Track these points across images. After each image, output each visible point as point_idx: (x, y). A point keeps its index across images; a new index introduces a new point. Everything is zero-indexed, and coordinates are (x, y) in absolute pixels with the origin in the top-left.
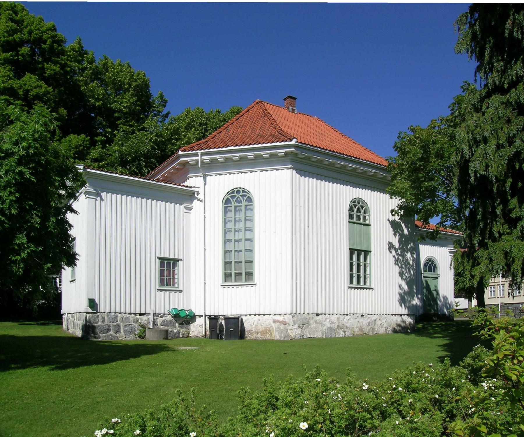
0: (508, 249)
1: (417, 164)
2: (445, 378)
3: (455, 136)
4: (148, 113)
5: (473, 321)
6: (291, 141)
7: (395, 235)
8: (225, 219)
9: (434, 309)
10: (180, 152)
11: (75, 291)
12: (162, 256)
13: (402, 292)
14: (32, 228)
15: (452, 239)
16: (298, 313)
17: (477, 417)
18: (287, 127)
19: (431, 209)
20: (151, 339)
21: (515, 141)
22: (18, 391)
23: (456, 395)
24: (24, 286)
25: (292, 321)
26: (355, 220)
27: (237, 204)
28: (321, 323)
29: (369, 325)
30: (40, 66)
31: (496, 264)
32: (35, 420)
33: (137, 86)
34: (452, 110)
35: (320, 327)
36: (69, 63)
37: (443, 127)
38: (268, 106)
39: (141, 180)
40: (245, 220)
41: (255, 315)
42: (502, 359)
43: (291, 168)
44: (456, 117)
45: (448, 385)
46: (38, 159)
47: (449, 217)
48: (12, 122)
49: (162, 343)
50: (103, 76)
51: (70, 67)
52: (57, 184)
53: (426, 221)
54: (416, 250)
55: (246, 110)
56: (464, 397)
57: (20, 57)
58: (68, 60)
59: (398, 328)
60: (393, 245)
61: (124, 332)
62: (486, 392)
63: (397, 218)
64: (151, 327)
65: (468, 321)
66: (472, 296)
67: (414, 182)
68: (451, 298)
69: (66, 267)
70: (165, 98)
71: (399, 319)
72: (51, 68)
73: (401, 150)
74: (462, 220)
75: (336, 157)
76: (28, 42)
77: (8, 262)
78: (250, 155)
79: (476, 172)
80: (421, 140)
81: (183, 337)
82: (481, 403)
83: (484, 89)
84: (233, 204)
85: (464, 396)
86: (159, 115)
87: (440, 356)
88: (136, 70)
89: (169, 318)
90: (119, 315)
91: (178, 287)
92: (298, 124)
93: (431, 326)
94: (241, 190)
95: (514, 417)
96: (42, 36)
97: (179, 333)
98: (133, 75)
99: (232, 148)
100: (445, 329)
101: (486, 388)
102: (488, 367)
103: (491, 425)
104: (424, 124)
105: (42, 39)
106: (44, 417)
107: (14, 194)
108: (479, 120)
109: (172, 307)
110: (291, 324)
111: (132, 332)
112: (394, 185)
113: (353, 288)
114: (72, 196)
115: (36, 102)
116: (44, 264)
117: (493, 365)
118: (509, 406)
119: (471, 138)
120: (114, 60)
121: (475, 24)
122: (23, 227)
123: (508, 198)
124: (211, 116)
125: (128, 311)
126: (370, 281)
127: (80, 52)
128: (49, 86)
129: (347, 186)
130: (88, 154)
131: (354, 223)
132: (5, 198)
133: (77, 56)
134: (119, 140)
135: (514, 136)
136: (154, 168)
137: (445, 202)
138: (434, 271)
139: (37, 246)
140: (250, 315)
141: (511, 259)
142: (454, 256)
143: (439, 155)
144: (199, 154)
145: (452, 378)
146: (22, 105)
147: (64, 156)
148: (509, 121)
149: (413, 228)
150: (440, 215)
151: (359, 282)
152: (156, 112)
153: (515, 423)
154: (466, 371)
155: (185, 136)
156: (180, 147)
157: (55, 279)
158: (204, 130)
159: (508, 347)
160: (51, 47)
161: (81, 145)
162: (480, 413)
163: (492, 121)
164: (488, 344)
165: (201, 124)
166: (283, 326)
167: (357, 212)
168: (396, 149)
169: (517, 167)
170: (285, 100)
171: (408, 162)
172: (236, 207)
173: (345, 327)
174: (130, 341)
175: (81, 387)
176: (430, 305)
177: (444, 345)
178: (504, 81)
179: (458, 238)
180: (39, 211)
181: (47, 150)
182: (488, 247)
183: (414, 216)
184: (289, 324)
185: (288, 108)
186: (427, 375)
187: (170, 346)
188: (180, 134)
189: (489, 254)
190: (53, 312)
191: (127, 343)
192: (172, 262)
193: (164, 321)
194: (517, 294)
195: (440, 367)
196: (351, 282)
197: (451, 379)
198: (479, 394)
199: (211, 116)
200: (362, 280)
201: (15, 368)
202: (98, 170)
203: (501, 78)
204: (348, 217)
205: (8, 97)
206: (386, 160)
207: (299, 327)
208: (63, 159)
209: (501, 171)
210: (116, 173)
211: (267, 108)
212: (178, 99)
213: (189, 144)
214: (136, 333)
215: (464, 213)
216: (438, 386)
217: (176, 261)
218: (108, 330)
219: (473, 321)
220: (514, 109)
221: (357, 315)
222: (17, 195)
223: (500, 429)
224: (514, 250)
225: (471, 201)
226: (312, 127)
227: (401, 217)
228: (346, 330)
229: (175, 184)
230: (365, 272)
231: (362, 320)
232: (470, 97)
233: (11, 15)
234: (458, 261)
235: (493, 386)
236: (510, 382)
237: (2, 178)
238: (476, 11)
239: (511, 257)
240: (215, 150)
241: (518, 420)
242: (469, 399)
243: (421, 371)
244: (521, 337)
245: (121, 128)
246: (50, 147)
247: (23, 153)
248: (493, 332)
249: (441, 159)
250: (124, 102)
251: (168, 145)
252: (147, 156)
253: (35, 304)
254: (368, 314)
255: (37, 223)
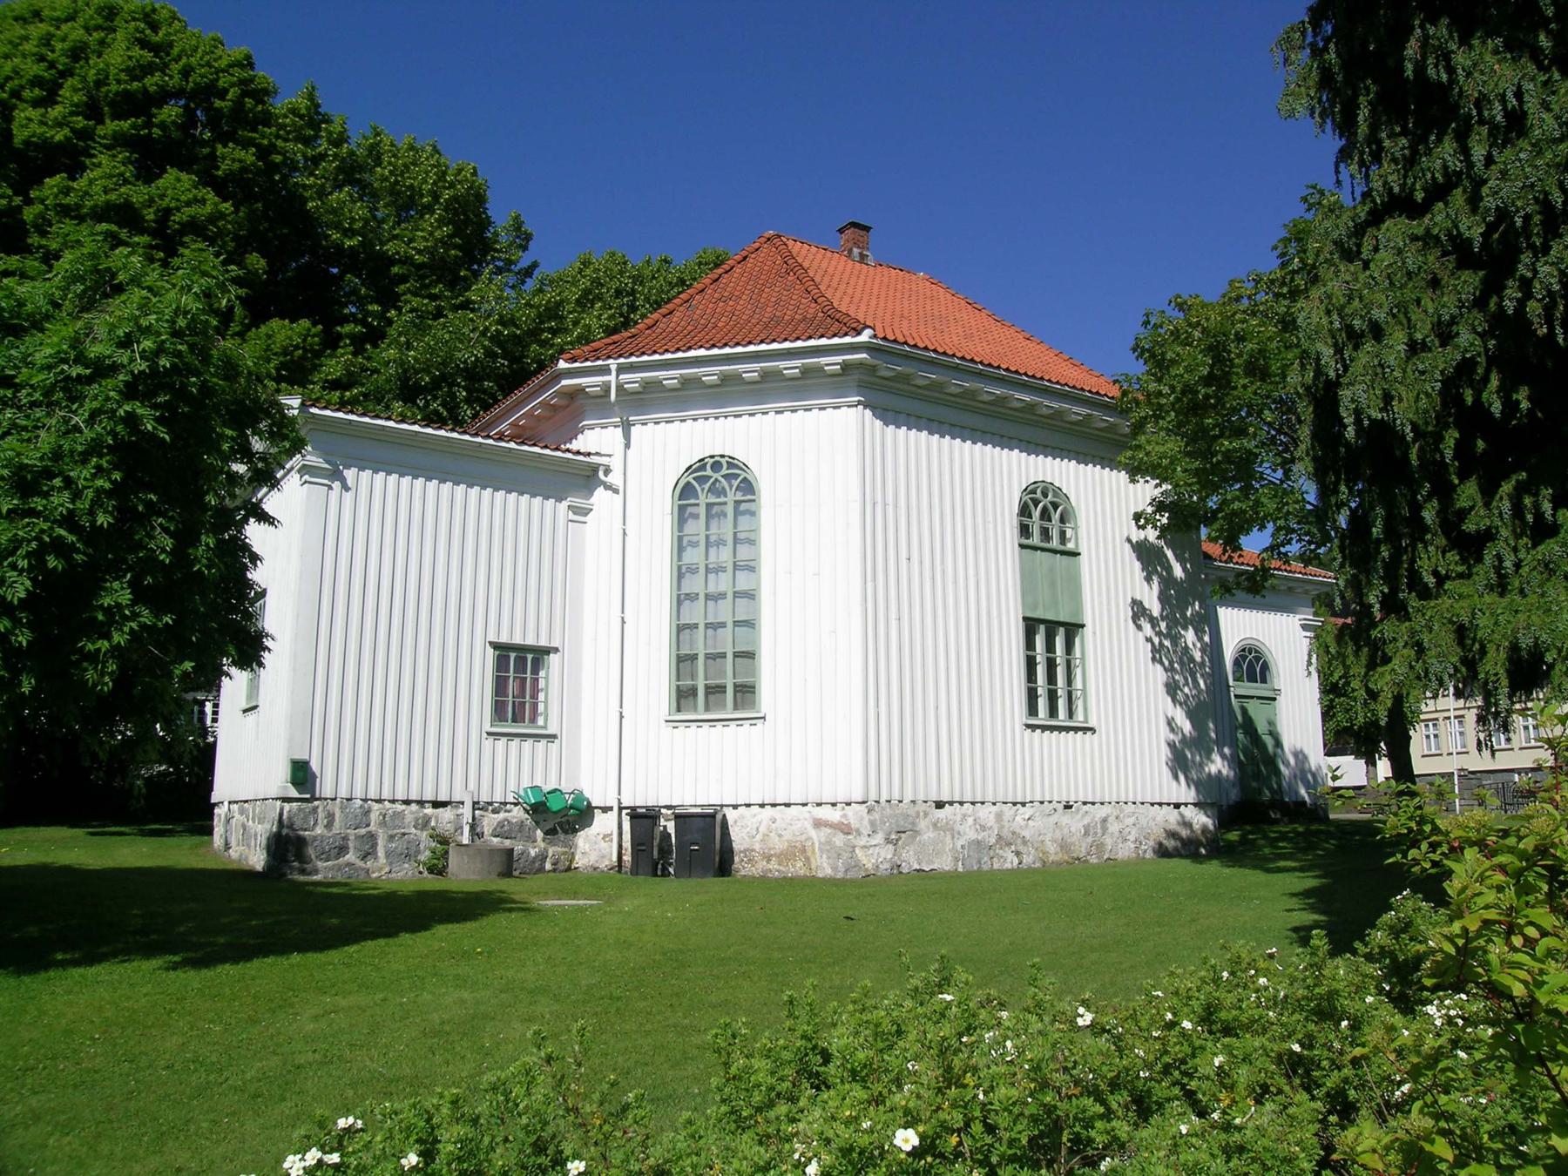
0: (1466, 620)
1: (1198, 392)
2: (1317, 990)
3: (1294, 321)
4: (480, 265)
5: (1384, 823)
6: (859, 334)
7: (1148, 579)
8: (680, 539)
9: (1270, 789)
10: (562, 365)
11: (253, 742)
12: (504, 639)
13: (1177, 739)
14: (150, 562)
15: (1306, 592)
16: (883, 800)
17: (1421, 1111)
18: (846, 299)
19: (1245, 512)
20: (464, 875)
21: (1458, 334)
22: (68, 1032)
23: (1353, 1044)
24: (114, 723)
25: (866, 822)
26: (1036, 540)
27: (712, 499)
28: (949, 829)
29: (1086, 833)
30: (206, 151)
31: (1434, 661)
32: (111, 1122)
33: (455, 199)
34: (1283, 255)
35: (948, 839)
36: (280, 143)
37: (1262, 297)
38: (796, 248)
39: (455, 435)
40: (736, 541)
41: (762, 806)
42: (1479, 935)
43: (859, 403)
44: (1294, 272)
45: (1326, 1012)
46: (182, 383)
47: (1293, 531)
48: (119, 289)
49: (493, 887)
50: (366, 176)
51: (284, 155)
52: (226, 447)
53: (1231, 542)
54: (1208, 623)
55: (738, 258)
56: (1376, 1050)
57: (155, 130)
58: (278, 137)
59: (1170, 844)
60: (1144, 609)
61: (388, 855)
62: (1438, 1035)
63: (1151, 534)
64: (465, 842)
65: (1369, 822)
66: (1377, 749)
67: (1192, 440)
68: (1317, 758)
69: (234, 671)
70: (527, 227)
71: (1171, 817)
72: (233, 157)
73: (1153, 356)
74: (1330, 540)
75: (980, 374)
76: (179, 94)
77: (73, 658)
78: (750, 371)
79: (1358, 413)
80: (1204, 331)
81: (554, 870)
82: (1427, 1065)
83: (1363, 202)
84: (703, 499)
85: (1375, 1047)
86: (509, 271)
87: (1297, 924)
88: (452, 161)
89: (517, 814)
90: (376, 806)
91: (545, 727)
92: (875, 292)
93: (1265, 837)
94: (723, 461)
95: (1530, 1111)
96: (217, 80)
97: (542, 857)
98: (444, 173)
99: (702, 352)
100: (1305, 844)
101: (1438, 1022)
102: (1439, 957)
103: (1464, 1137)
104: (1212, 292)
105: (215, 87)
106: (137, 1115)
107: (109, 472)
108: (1356, 280)
109: (526, 783)
110: (866, 833)
111: (409, 855)
112: (1139, 447)
113: (1038, 727)
114: (266, 477)
115: (186, 239)
116: (173, 662)
117: (1452, 951)
118: (1511, 1078)
119: (1337, 325)
120: (398, 136)
121: (1326, 49)
122: (125, 561)
123: (1451, 482)
124: (647, 272)
125: (400, 796)
126: (1085, 709)
127: (311, 118)
128: (225, 201)
129: (1011, 449)
130: (316, 368)
131: (1035, 548)
132: (81, 483)
133: (301, 127)
134: (400, 335)
135: (1453, 321)
136: (492, 406)
137: (1281, 493)
138: (1264, 681)
139: (157, 614)
140: (748, 805)
141: (1477, 646)
142: (1317, 637)
143: (1257, 369)
144: (613, 368)
145: (1337, 992)
146: (151, 247)
147: (250, 373)
148: (1435, 283)
149: (1198, 560)
150: (1270, 527)
151: (1053, 712)
152: (500, 264)
153: (1533, 1130)
154: (1374, 970)
155: (576, 323)
156: (562, 351)
157: (202, 704)
158: (627, 307)
159: (1491, 897)
160: (238, 103)
161: (297, 347)
162: (1429, 1098)
163: (1392, 283)
164: (1433, 888)
165: (618, 293)
166: (841, 836)
167: (1042, 519)
168: (1141, 355)
169: (1469, 400)
170: (841, 231)
171: (1173, 388)
172: (709, 506)
173: (1019, 841)
174: (401, 881)
175: (253, 1021)
176: (1257, 776)
177: (1307, 894)
178: (1414, 184)
179: (1325, 589)
180: (171, 519)
181: (206, 359)
182: (1407, 613)
183: (1198, 529)
184: (859, 833)
185: (850, 251)
186: (1262, 981)
187: (517, 897)
188: (562, 318)
189: (1413, 633)
190: (187, 798)
191: (394, 887)
192: (530, 657)
193: (501, 824)
194: (1503, 746)
195: (1299, 959)
196: (1032, 710)
197: (1332, 995)
198: (1419, 1039)
199: (647, 272)
200: (1062, 704)
201: (64, 964)
202: (338, 410)
203: (1405, 177)
204: (1016, 531)
205: (114, 228)
206: (1115, 382)
207: (888, 841)
208: (248, 381)
209: (1426, 411)
210: (389, 418)
211: (794, 253)
212: (560, 232)
213: (587, 343)
214: (422, 858)
215: (1335, 521)
216: (1296, 1016)
217: (537, 656)
218: (342, 850)
219: (1384, 823)
220: (1445, 254)
221: (1051, 806)
222: (117, 476)
223: (1489, 1149)
224: (1483, 621)
225: (1350, 490)
226: (914, 298)
227: (1164, 532)
228: (1021, 848)
229: (546, 447)
230: (1069, 682)
231: (1065, 819)
232: (1327, 224)
233: (142, 32)
234: (1328, 652)
235: (1458, 1016)
236: (1507, 1005)
237: (81, 432)
238: (1327, 19)
239: (1474, 640)
240: (656, 357)
241: (1542, 1120)
242: (1392, 1057)
243: (1245, 970)
244: (1526, 869)
245: (407, 302)
246: (214, 352)
247: (141, 366)
248: (1443, 854)
249: (1263, 380)
250: (421, 237)
251: (529, 345)
252: (473, 374)
253: (139, 777)
254: (1085, 803)
255: (163, 550)
